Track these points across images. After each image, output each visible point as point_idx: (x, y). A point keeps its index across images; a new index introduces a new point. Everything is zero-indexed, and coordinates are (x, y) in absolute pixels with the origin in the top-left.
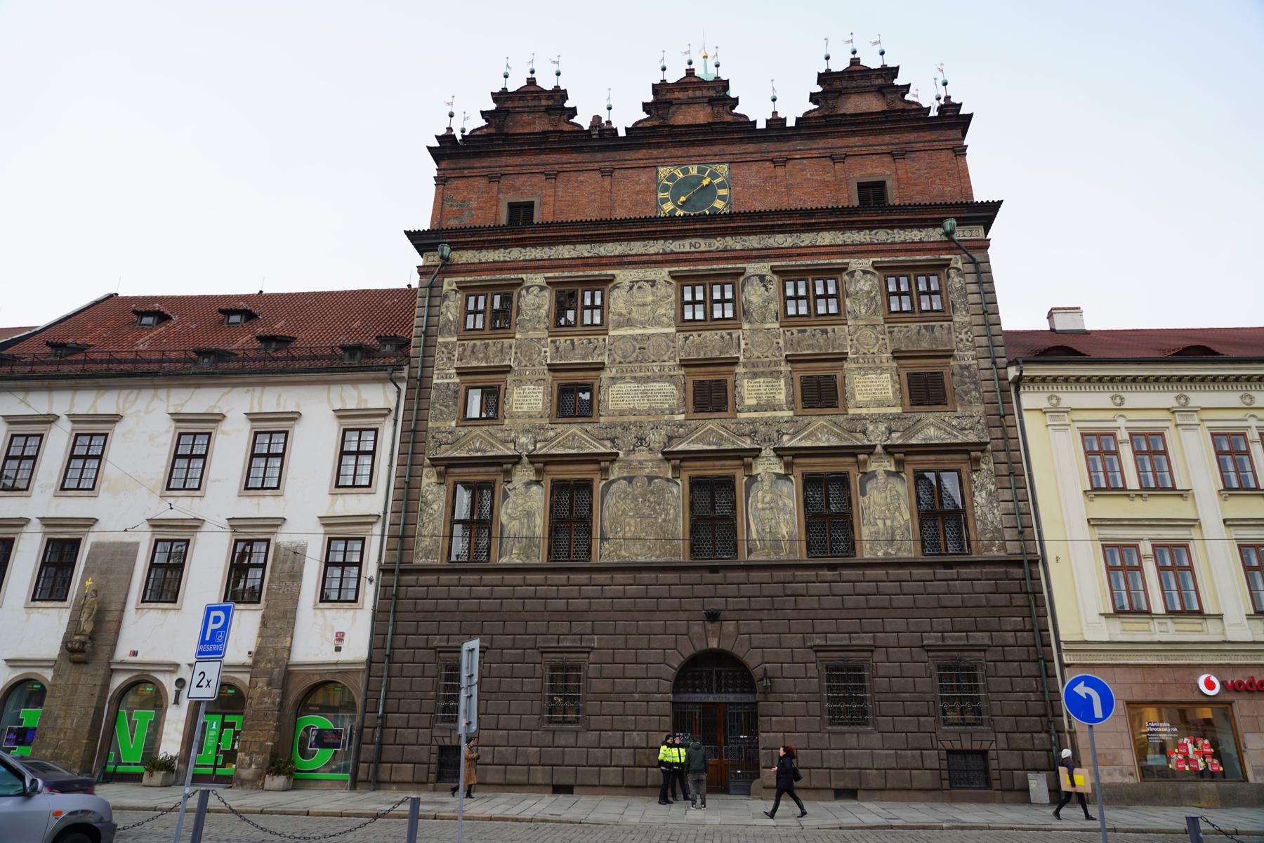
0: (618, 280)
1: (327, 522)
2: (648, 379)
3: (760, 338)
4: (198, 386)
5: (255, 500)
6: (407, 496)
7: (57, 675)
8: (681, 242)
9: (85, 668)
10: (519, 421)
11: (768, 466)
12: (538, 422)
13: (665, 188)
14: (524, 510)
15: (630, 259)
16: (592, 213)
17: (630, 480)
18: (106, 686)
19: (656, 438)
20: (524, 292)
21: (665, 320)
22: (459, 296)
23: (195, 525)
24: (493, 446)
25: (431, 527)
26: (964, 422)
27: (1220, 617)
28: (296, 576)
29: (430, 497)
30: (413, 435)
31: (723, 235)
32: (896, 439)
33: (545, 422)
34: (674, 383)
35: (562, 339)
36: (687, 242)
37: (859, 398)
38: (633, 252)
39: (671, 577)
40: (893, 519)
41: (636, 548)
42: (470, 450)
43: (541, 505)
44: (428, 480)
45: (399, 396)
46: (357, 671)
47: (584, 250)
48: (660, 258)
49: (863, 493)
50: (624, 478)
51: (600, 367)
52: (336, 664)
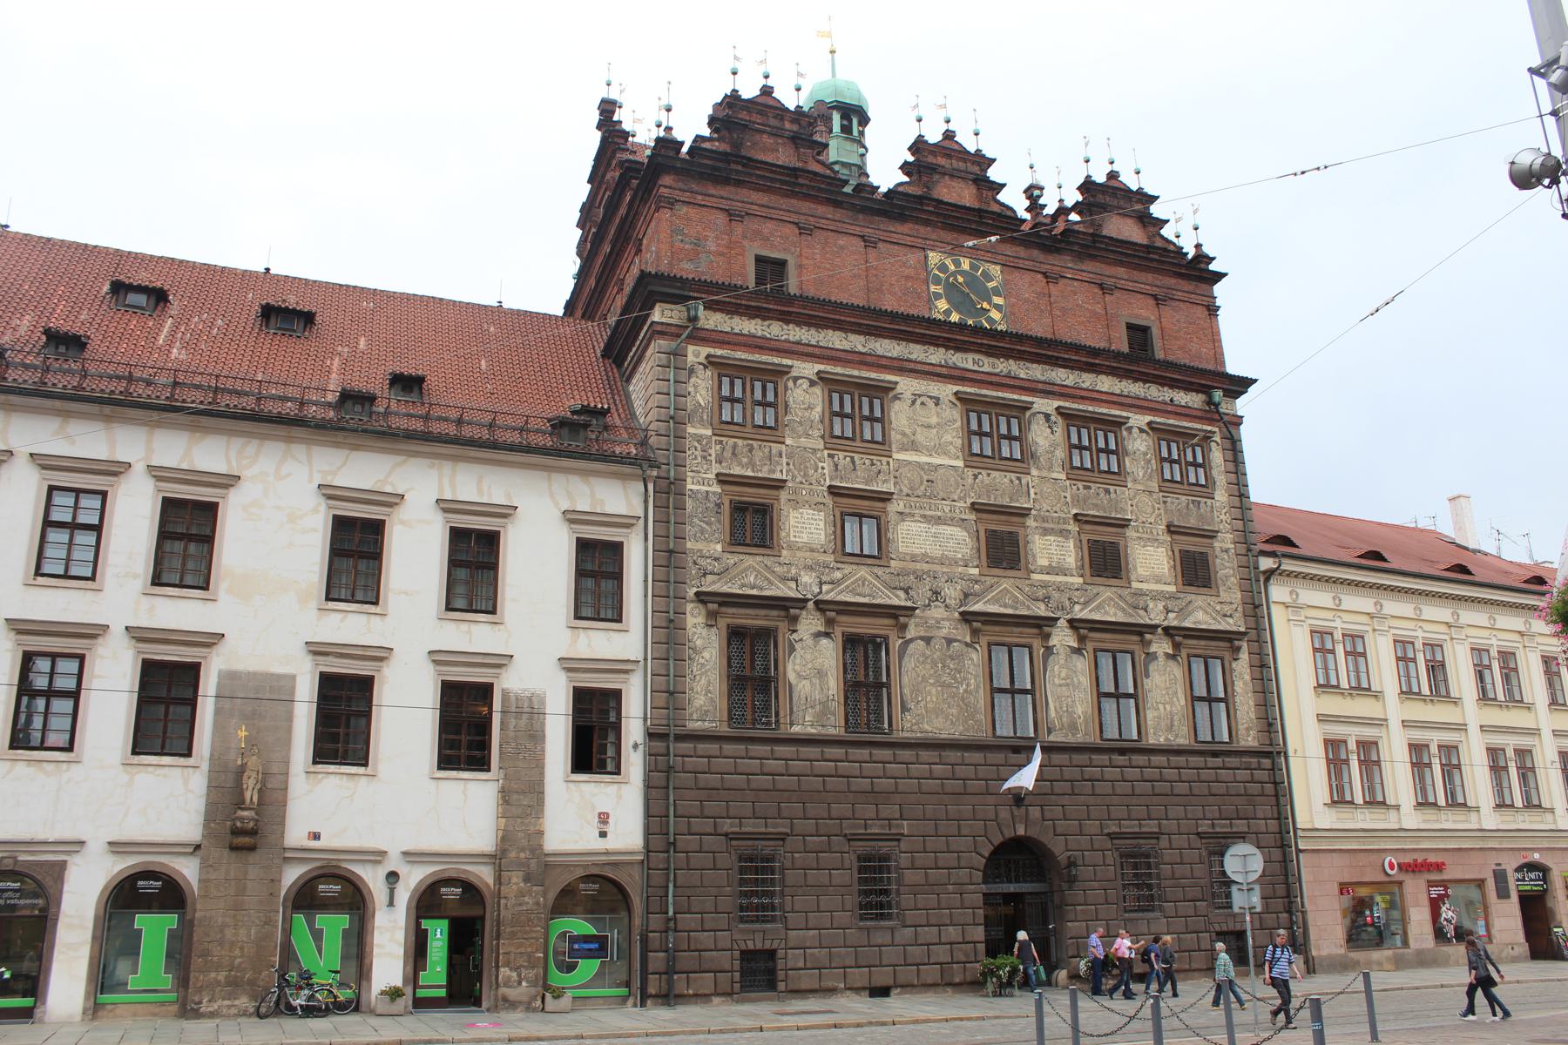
0: (899, 389)
1: (569, 665)
2: (939, 521)
3: (1047, 488)
4: (356, 448)
5: (464, 627)
6: (668, 639)
7: (205, 866)
8: (964, 356)
9: (253, 857)
10: (799, 554)
11: (1062, 638)
12: (822, 558)
13: (937, 281)
14: (812, 670)
15: (912, 366)
16: (854, 295)
17: (928, 640)
18: (276, 882)
19: (952, 593)
20: (790, 384)
21: (953, 450)
22: (709, 373)
23: (381, 655)
24: (770, 583)
25: (703, 681)
26: (1226, 608)
27: (1397, 807)
28: (537, 736)
29: (699, 642)
30: (669, 558)
31: (1007, 357)
32: (1172, 620)
33: (830, 558)
34: (965, 529)
35: (841, 455)
36: (970, 356)
37: (1140, 571)
38: (913, 357)
39: (977, 757)
40: (1172, 704)
42: (743, 585)
43: (833, 663)
44: (694, 619)
45: (646, 501)
46: (631, 863)
47: (857, 342)
48: (944, 371)
49: (1147, 676)
50: (922, 638)
51: (885, 498)
52: (607, 853)
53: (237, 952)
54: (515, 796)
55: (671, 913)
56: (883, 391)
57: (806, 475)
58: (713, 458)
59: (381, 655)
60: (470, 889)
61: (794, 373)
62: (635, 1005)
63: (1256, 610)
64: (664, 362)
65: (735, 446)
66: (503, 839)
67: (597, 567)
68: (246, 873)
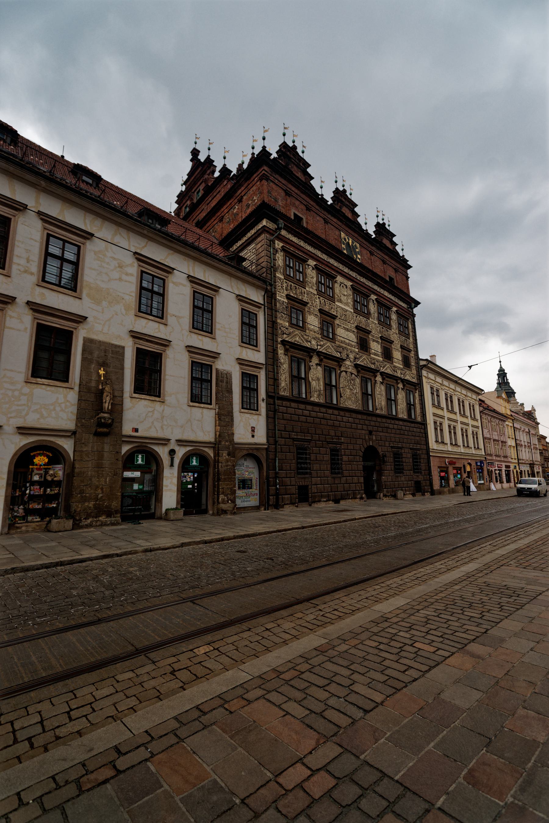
0: (336, 279)
1: (241, 362)
5: (200, 337)
9: (107, 440)
10: (311, 333)
12: (317, 336)
17: (346, 372)
18: (118, 452)
19: (352, 356)
20: (307, 266)
23: (166, 344)
25: (284, 376)
28: (230, 391)
29: (282, 361)
30: (272, 325)
35: (322, 298)
41: (350, 402)
42: (295, 341)
43: (322, 376)
44: (281, 351)
46: (263, 449)
52: (256, 444)
53: (99, 491)
54: (223, 417)
55: (277, 470)
56: (332, 278)
57: (312, 303)
58: (284, 288)
59: (166, 344)
60: (203, 459)
61: (308, 263)
62: (265, 510)
63: (420, 377)
64: (268, 244)
65: (291, 286)
66: (219, 435)
67: (248, 324)
68: (103, 448)
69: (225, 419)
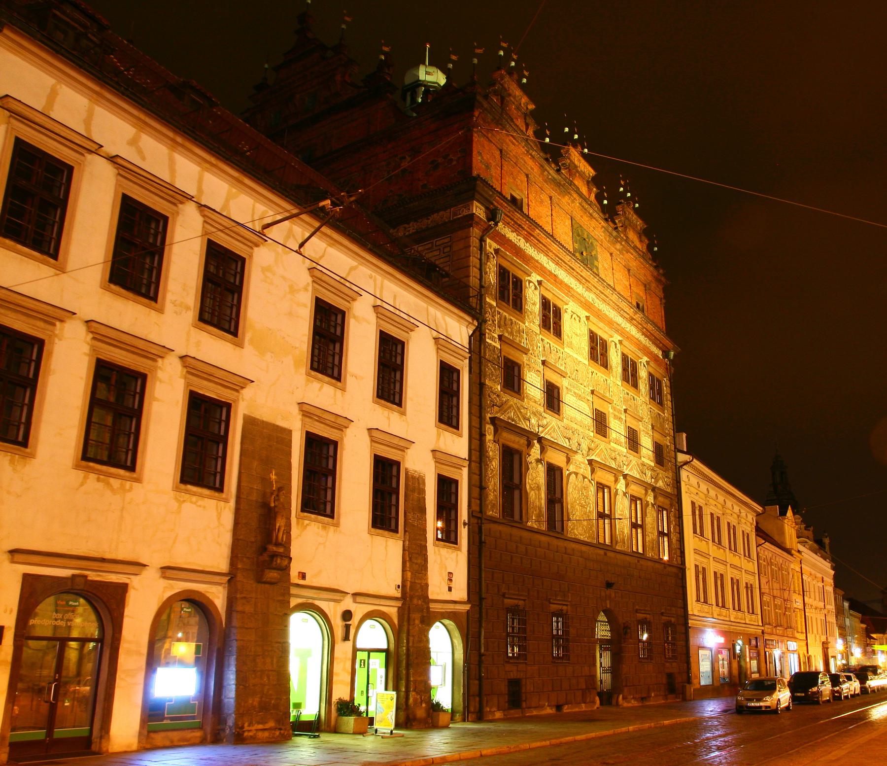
5: (386, 412)
17: (576, 474)
19: (584, 446)
42: (509, 418)
69: (415, 560)
